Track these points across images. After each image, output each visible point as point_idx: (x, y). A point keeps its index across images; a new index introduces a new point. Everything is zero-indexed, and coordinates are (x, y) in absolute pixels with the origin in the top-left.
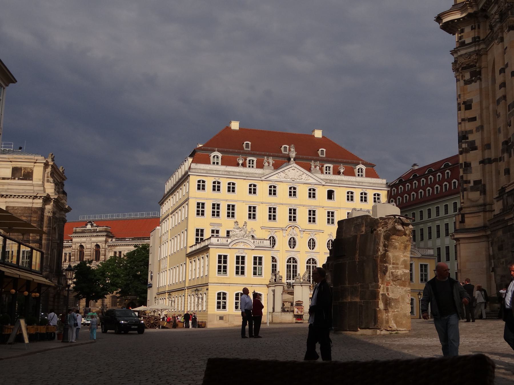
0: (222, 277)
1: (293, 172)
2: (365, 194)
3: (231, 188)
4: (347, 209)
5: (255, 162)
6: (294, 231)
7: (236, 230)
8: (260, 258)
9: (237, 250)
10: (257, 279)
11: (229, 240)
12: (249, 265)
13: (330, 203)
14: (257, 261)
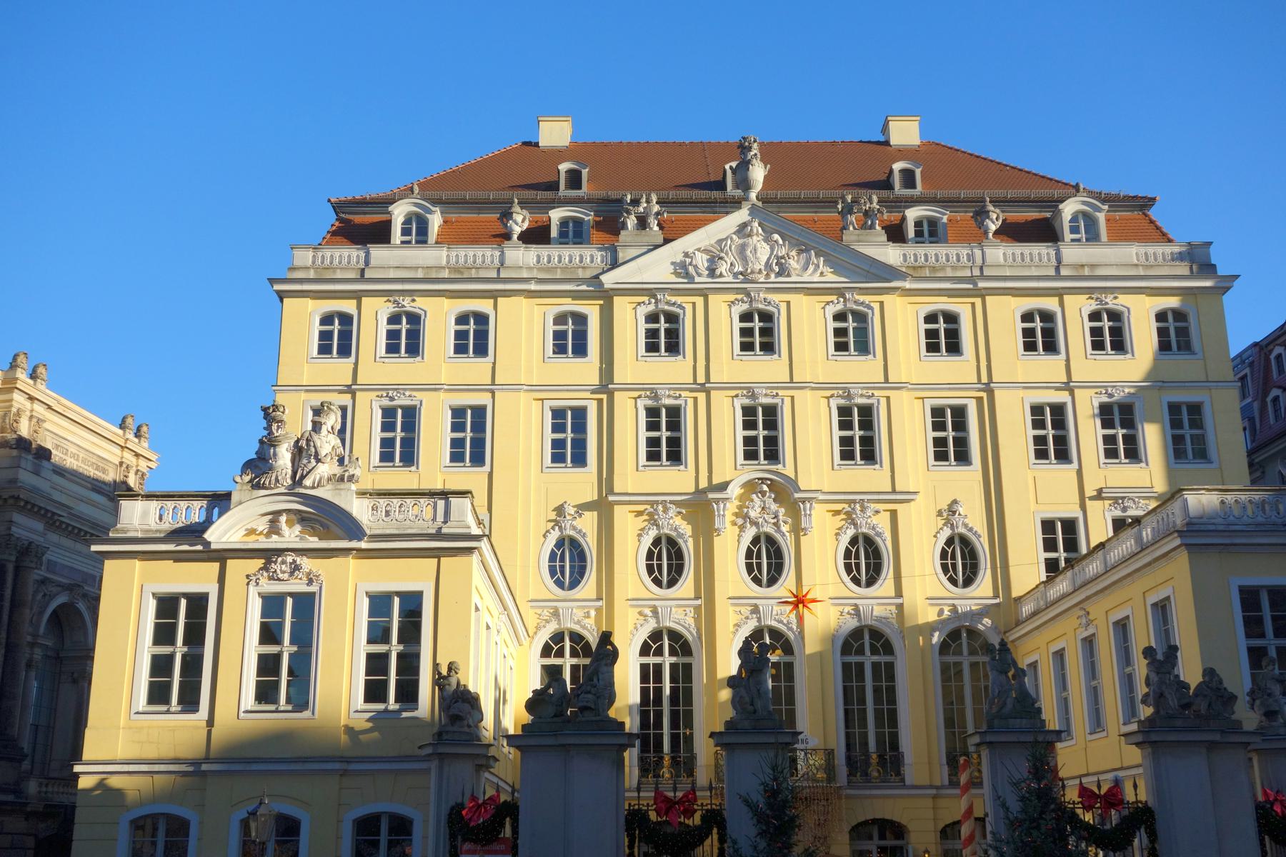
2: (1115, 316)
3: (474, 337)
13: (945, 368)
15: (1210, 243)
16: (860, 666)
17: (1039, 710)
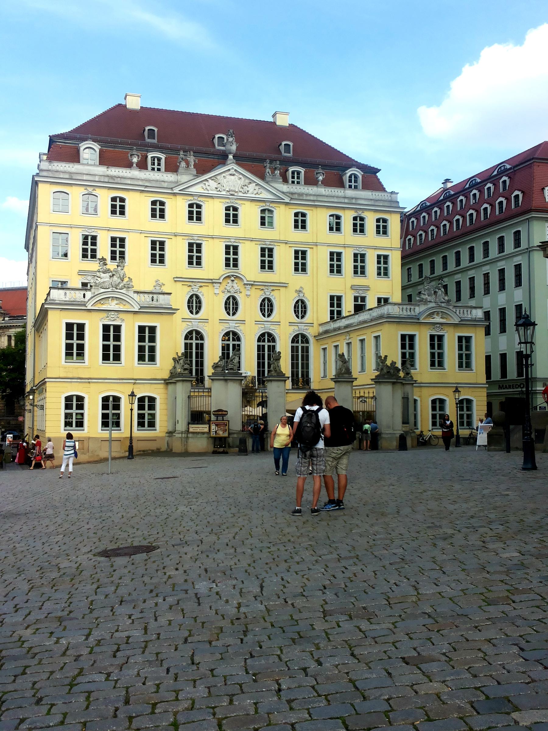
0: (74, 368)
1: (232, 179)
2: (362, 219)
4: (329, 245)
5: (163, 162)
6: (235, 285)
7: (102, 275)
8: (153, 329)
9: (104, 315)
10: (146, 370)
11: (89, 294)
12: (129, 343)
13: (299, 236)
14: (147, 334)
15: (398, 193)
16: (264, 346)
17: (351, 372)
